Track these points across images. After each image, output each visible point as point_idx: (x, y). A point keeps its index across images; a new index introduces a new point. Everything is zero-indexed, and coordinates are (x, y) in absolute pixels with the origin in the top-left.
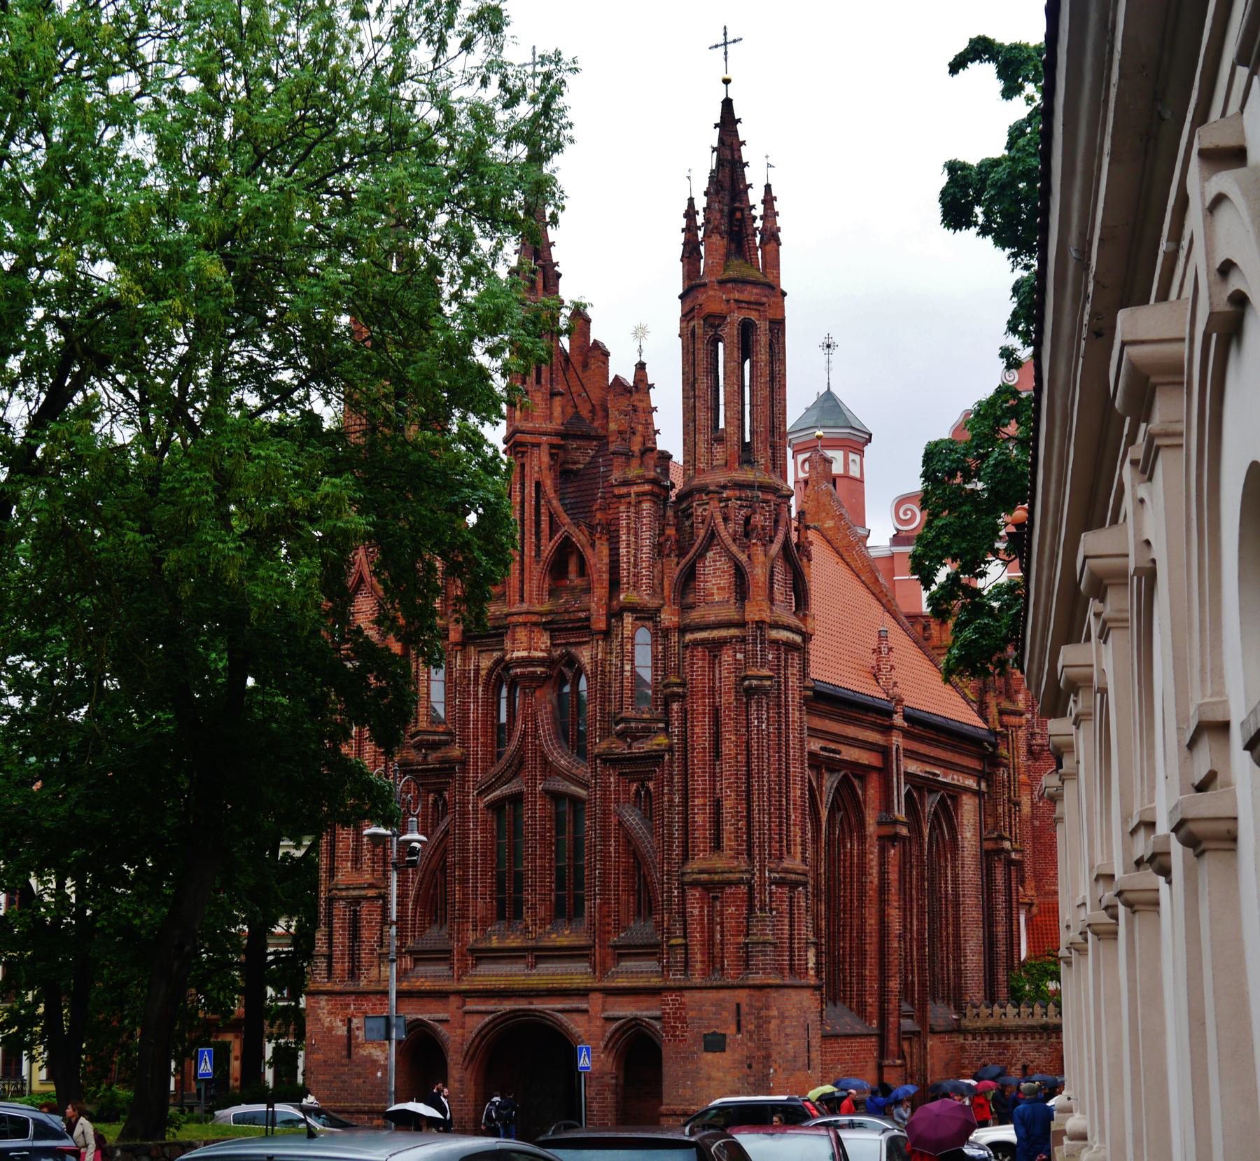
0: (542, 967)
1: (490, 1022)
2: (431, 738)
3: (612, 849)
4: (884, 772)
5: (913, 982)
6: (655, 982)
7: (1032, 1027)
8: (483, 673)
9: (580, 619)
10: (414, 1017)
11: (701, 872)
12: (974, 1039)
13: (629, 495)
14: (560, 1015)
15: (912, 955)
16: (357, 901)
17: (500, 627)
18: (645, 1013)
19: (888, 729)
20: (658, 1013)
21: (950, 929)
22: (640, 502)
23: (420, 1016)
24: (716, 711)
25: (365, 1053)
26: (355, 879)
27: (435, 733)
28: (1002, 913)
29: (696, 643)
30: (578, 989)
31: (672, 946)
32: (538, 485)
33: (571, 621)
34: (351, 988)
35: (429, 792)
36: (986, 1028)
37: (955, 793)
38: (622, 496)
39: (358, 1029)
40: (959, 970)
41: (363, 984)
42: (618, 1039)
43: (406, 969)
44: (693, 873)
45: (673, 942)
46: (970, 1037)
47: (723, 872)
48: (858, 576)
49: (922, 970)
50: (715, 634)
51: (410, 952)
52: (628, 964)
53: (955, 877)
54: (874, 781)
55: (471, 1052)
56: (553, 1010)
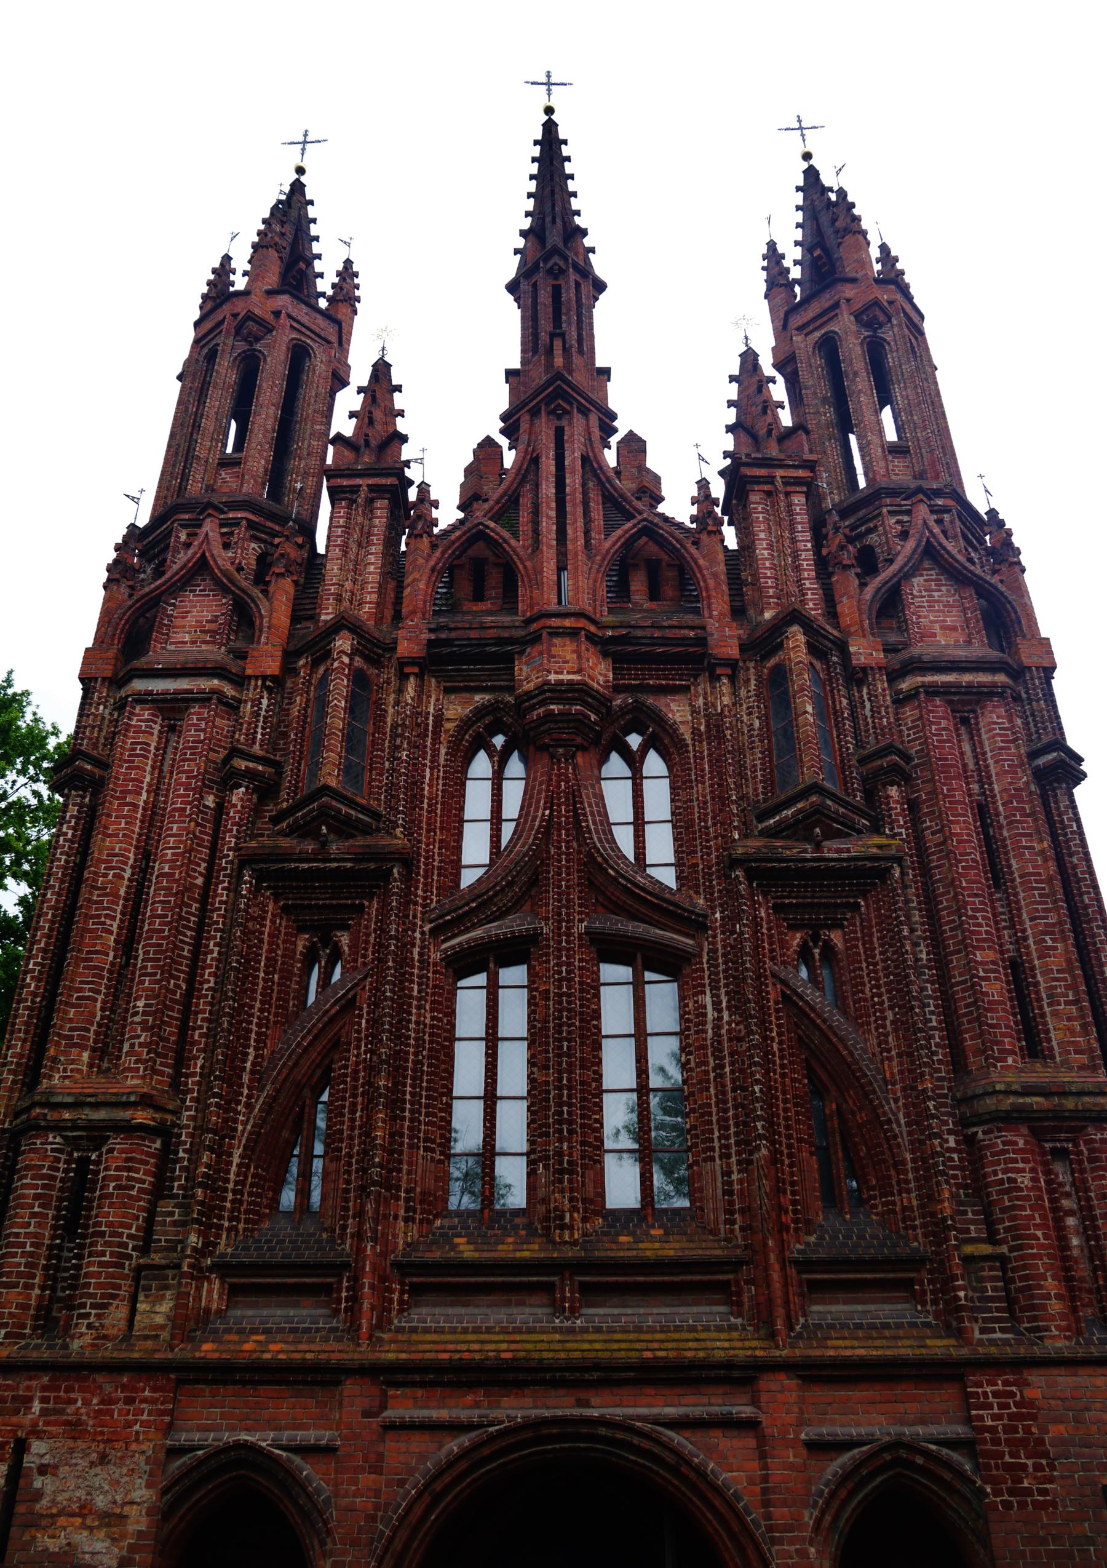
0: (600, 1313)
1: (465, 1453)
2: (344, 809)
3: (775, 1046)
6: (939, 1346)
8: (449, 726)
9: (683, 641)
10: (227, 1437)
11: (1027, 1091)
13: (771, 480)
14: (676, 1437)
16: (97, 1135)
17: (511, 641)
18: (920, 1430)
20: (960, 1430)
22: (787, 494)
23: (244, 1437)
24: (983, 811)
25: (52, 1545)
26: (100, 1086)
27: (351, 803)
29: (933, 691)
30: (729, 1365)
31: (968, 1259)
32: (585, 459)
33: (665, 641)
34: (46, 1355)
35: (301, 930)
38: (757, 480)
39: (43, 1470)
41: (80, 1343)
42: (844, 1503)
43: (207, 1310)
44: (1007, 1093)
45: (969, 1249)
47: (1081, 1094)
50: (967, 678)
51: (223, 1268)
52: (834, 1308)
55: (398, 1545)
56: (656, 1421)
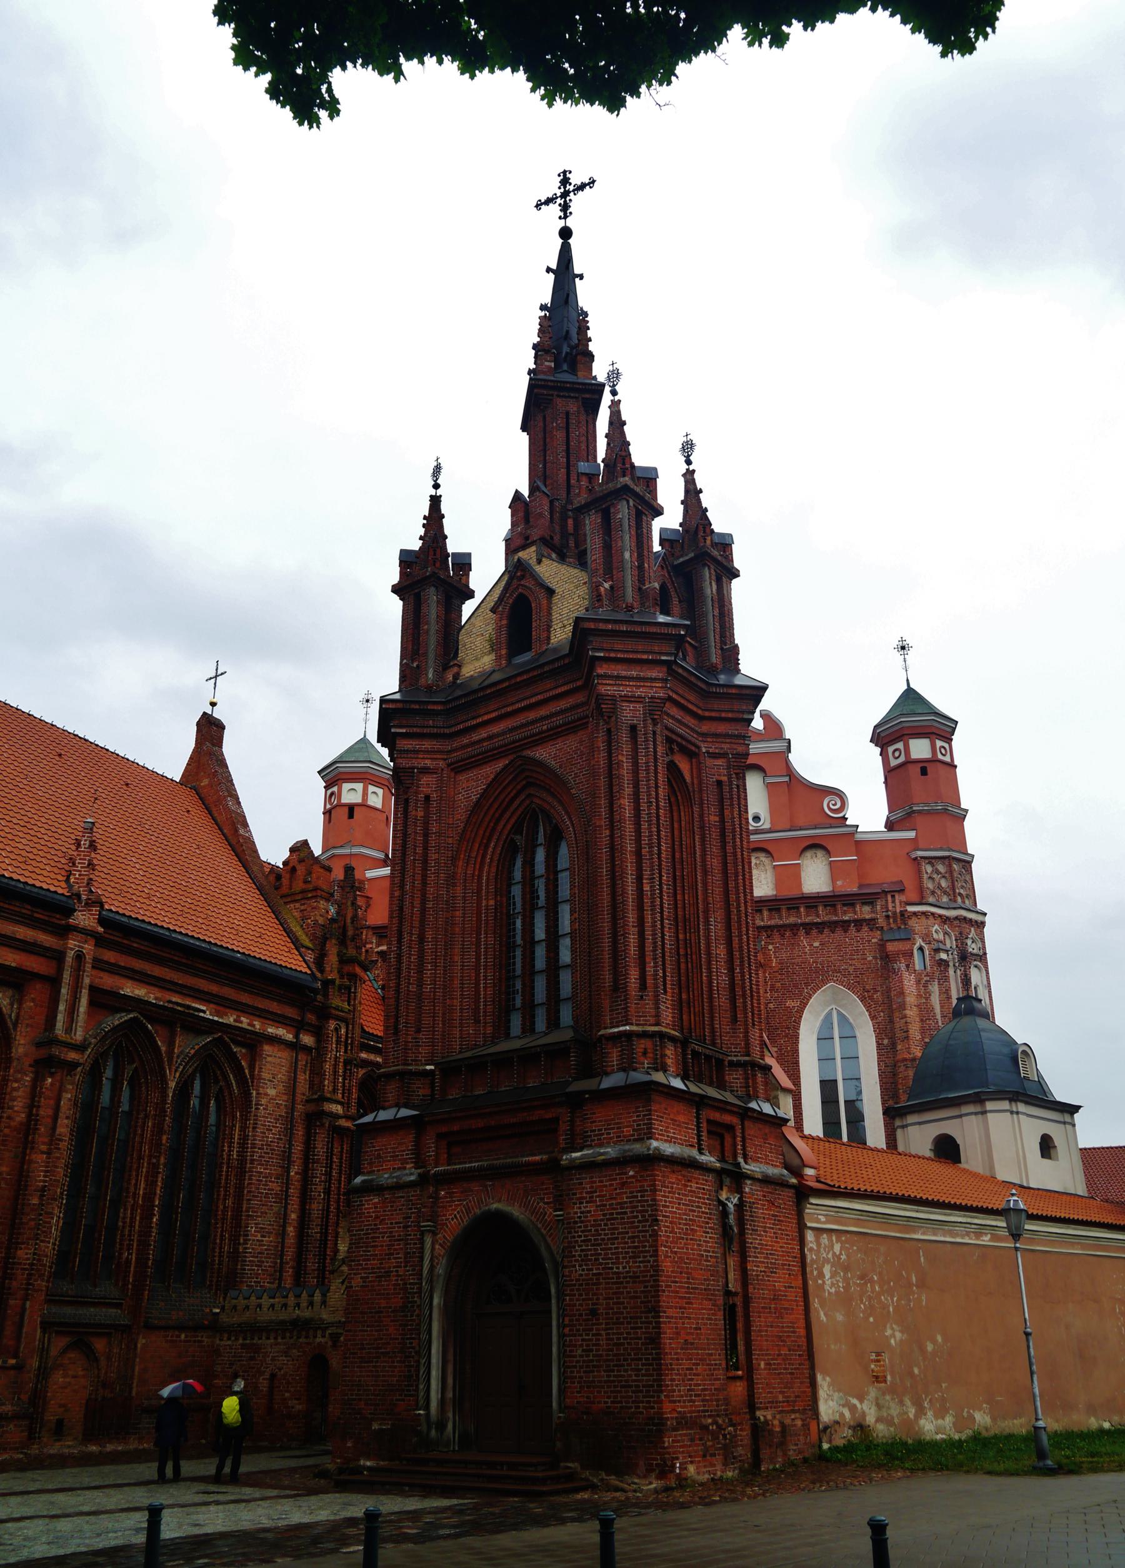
4: (54, 982)
5: (128, 1261)
7: (283, 1322)
12: (229, 1339)
15: (132, 1226)
19: (65, 931)
21: (229, 1202)
28: (320, 1188)
36: (240, 1325)
37: (254, 1042)
40: (236, 1251)
46: (226, 1336)
48: (220, 829)
49: (144, 1244)
53: (244, 1138)
54: (36, 993)
